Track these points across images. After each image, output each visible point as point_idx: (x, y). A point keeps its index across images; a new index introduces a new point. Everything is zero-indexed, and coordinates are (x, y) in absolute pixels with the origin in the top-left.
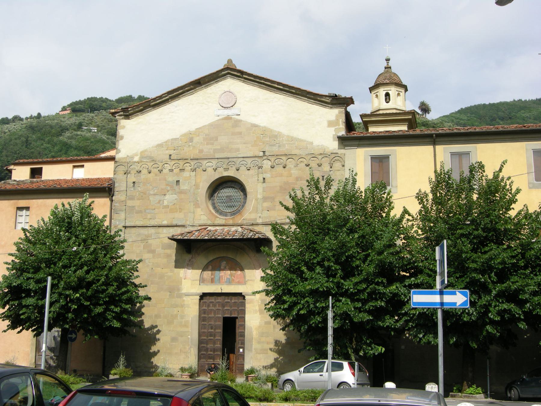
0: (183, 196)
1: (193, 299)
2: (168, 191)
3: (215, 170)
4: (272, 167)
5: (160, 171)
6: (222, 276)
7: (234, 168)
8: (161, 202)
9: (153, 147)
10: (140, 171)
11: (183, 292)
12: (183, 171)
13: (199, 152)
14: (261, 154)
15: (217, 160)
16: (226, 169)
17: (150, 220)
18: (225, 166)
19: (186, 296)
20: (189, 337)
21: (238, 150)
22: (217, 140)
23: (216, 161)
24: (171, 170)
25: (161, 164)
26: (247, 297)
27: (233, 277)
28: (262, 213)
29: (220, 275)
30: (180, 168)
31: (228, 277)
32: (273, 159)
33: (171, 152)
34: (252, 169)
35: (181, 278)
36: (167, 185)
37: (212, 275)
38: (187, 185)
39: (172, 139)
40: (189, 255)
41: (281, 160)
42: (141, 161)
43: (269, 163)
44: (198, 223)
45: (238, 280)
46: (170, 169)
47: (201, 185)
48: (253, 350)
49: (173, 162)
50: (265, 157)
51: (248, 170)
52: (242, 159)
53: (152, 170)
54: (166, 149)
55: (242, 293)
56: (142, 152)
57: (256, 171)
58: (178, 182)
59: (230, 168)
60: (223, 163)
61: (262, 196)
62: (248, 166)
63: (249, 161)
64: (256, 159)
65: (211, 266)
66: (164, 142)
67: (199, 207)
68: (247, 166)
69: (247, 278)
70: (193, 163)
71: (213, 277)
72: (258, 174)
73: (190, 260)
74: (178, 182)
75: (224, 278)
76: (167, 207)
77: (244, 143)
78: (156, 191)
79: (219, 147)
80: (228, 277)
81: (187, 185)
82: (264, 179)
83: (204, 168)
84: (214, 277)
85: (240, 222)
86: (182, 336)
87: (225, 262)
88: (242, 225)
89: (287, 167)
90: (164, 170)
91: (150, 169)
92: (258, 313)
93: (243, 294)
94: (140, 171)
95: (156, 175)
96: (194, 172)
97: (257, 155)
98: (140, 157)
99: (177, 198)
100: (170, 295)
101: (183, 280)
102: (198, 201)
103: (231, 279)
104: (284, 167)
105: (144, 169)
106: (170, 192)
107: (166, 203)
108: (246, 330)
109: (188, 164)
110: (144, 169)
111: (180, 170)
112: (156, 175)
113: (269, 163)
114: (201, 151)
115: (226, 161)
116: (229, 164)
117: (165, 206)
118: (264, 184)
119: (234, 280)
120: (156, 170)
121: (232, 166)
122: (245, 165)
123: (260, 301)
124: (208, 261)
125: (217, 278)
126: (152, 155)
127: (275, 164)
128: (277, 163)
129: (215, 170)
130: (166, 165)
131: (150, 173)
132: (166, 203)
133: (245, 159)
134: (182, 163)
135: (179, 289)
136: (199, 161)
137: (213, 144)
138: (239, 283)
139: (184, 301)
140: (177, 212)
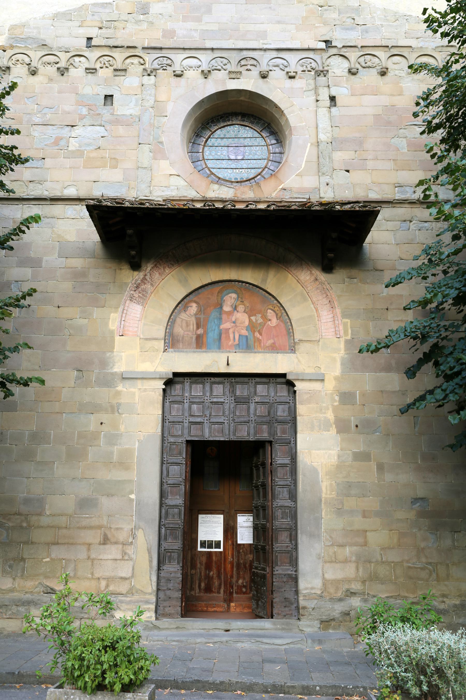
0: (121, 130)
1: (145, 390)
2: (82, 118)
3: (206, 74)
4: (352, 72)
5: (62, 72)
6: (227, 330)
7: (255, 72)
8: (62, 143)
9: (43, 18)
10: (8, 68)
11: (116, 369)
12: (123, 73)
13: (163, 36)
14: (323, 45)
15: (209, 52)
16: (235, 75)
17: (31, 185)
18: (233, 67)
19: (128, 383)
20: (133, 496)
21: (263, 35)
22: (209, 11)
23: (210, 55)
24: (91, 71)
25: (64, 58)
26: (299, 386)
27: (257, 334)
28: (331, 177)
29: (222, 327)
30: (115, 67)
31: (244, 332)
32: (353, 55)
33: (93, 32)
34: (300, 78)
35: (112, 332)
36: (80, 103)
37: (198, 328)
38: (132, 105)
39: (95, 5)
40: (136, 273)
41: (376, 60)
42: (12, 47)
43: (345, 65)
44: (163, 194)
45: (270, 342)
46: (88, 66)
47: (170, 107)
48: (324, 535)
49: (97, 53)
50: (333, 51)
51: (291, 77)
52: (274, 54)
53: (42, 69)
54: (78, 24)
55: (284, 375)
56: (13, 28)
57: (312, 82)
58: (109, 98)
59: (244, 72)
60: (225, 61)
61: (328, 135)
62: (292, 69)
63: (293, 58)
64: (311, 54)
65: (194, 305)
66: (75, 10)
67: (165, 157)
68: (287, 70)
69: (298, 336)
70: (149, 58)
71: (200, 331)
72: (316, 88)
73: (137, 287)
74: (109, 98)
75: (231, 336)
76: (79, 153)
77: (279, 22)
78: (48, 116)
79: (215, 27)
80: (244, 332)
81: (132, 105)
82: (333, 99)
83: (177, 68)
84: (206, 332)
85: (274, 195)
86: (110, 495)
87: (234, 295)
88: (281, 202)
89: (390, 74)
90: (72, 70)
91: (34, 64)
92: (333, 430)
93: (289, 377)
94: (8, 68)
95: (51, 80)
96: (152, 77)
97: (311, 47)
98: (9, 38)
99: (106, 134)
100: (78, 378)
101: (117, 338)
102: (161, 143)
103: (251, 338)
104: (383, 73)
105: (19, 66)
106: (87, 121)
107: (74, 145)
108: (300, 478)
109: (136, 60)
110: (19, 66)
111: (116, 70)
112: (51, 80)
113: (345, 65)
114: (171, 33)
115: (235, 57)
116: (243, 62)
117: (73, 152)
118: (333, 109)
119: (259, 341)
120: (52, 70)
121: (249, 67)
122: (281, 66)
123: (337, 398)
124: (189, 291)
125: (212, 335)
126: (42, 37)
127: (358, 66)
128: (364, 65)
129: (206, 74)
130: (77, 59)
131: (34, 73)
132: (74, 145)
133: (282, 55)
134: (119, 55)
135: (104, 363)
136: (164, 53)
137: (199, 20)
138: (274, 349)
139: (118, 393)
140: (105, 166)
